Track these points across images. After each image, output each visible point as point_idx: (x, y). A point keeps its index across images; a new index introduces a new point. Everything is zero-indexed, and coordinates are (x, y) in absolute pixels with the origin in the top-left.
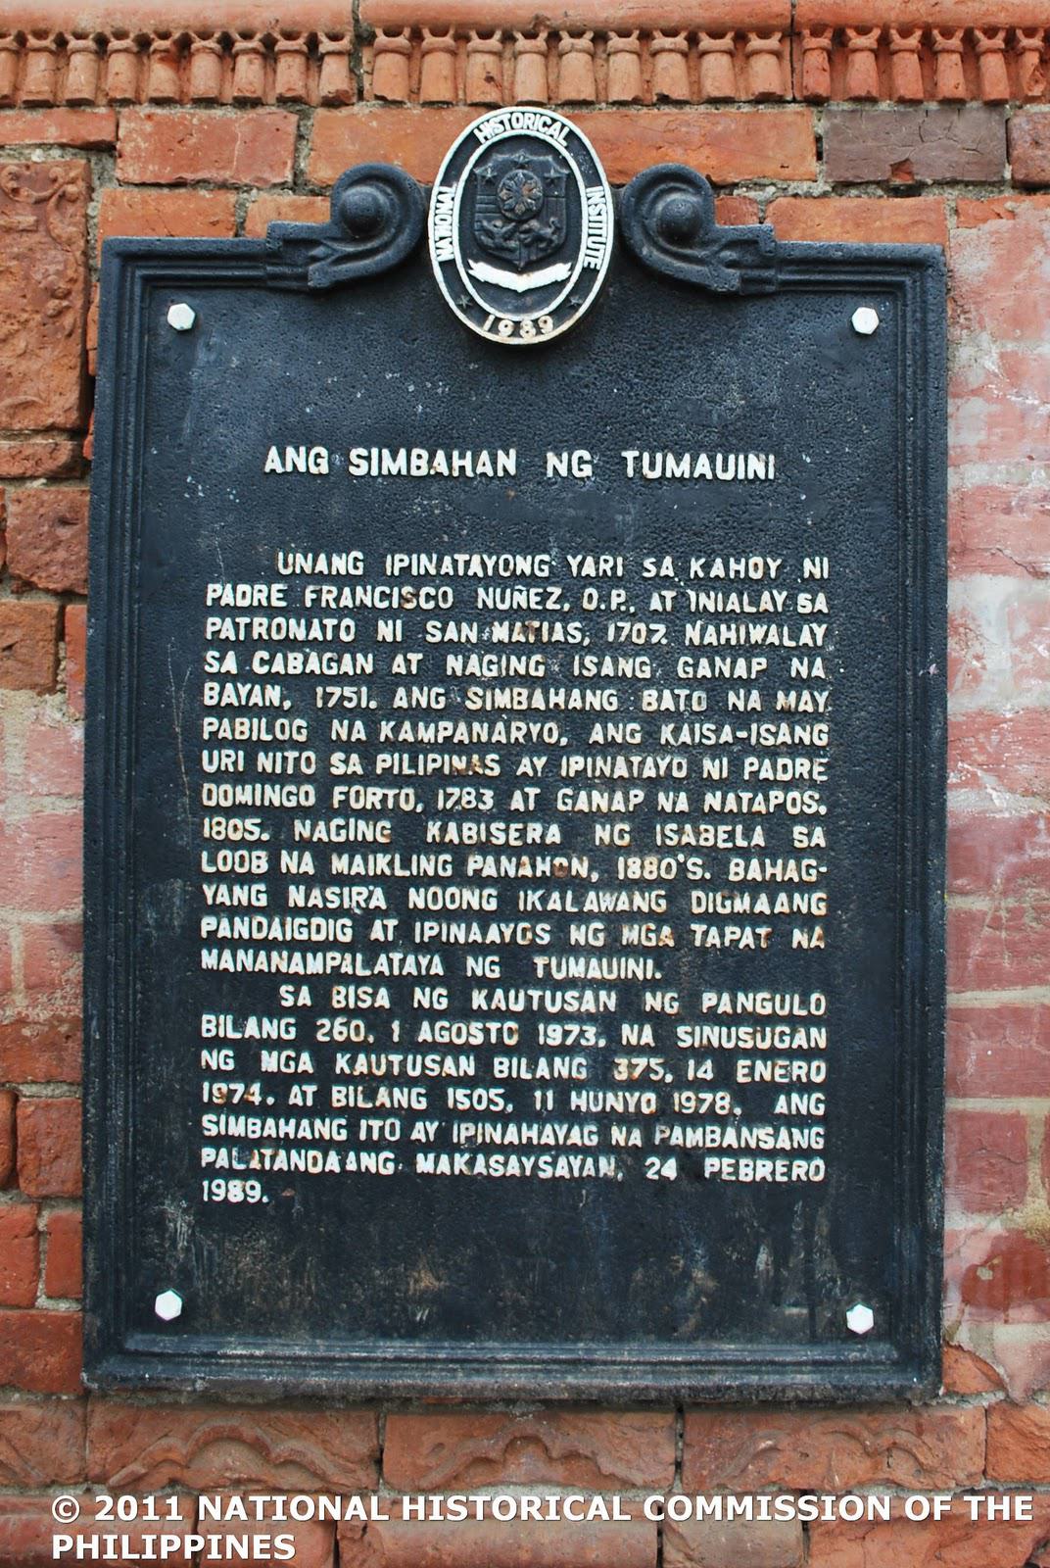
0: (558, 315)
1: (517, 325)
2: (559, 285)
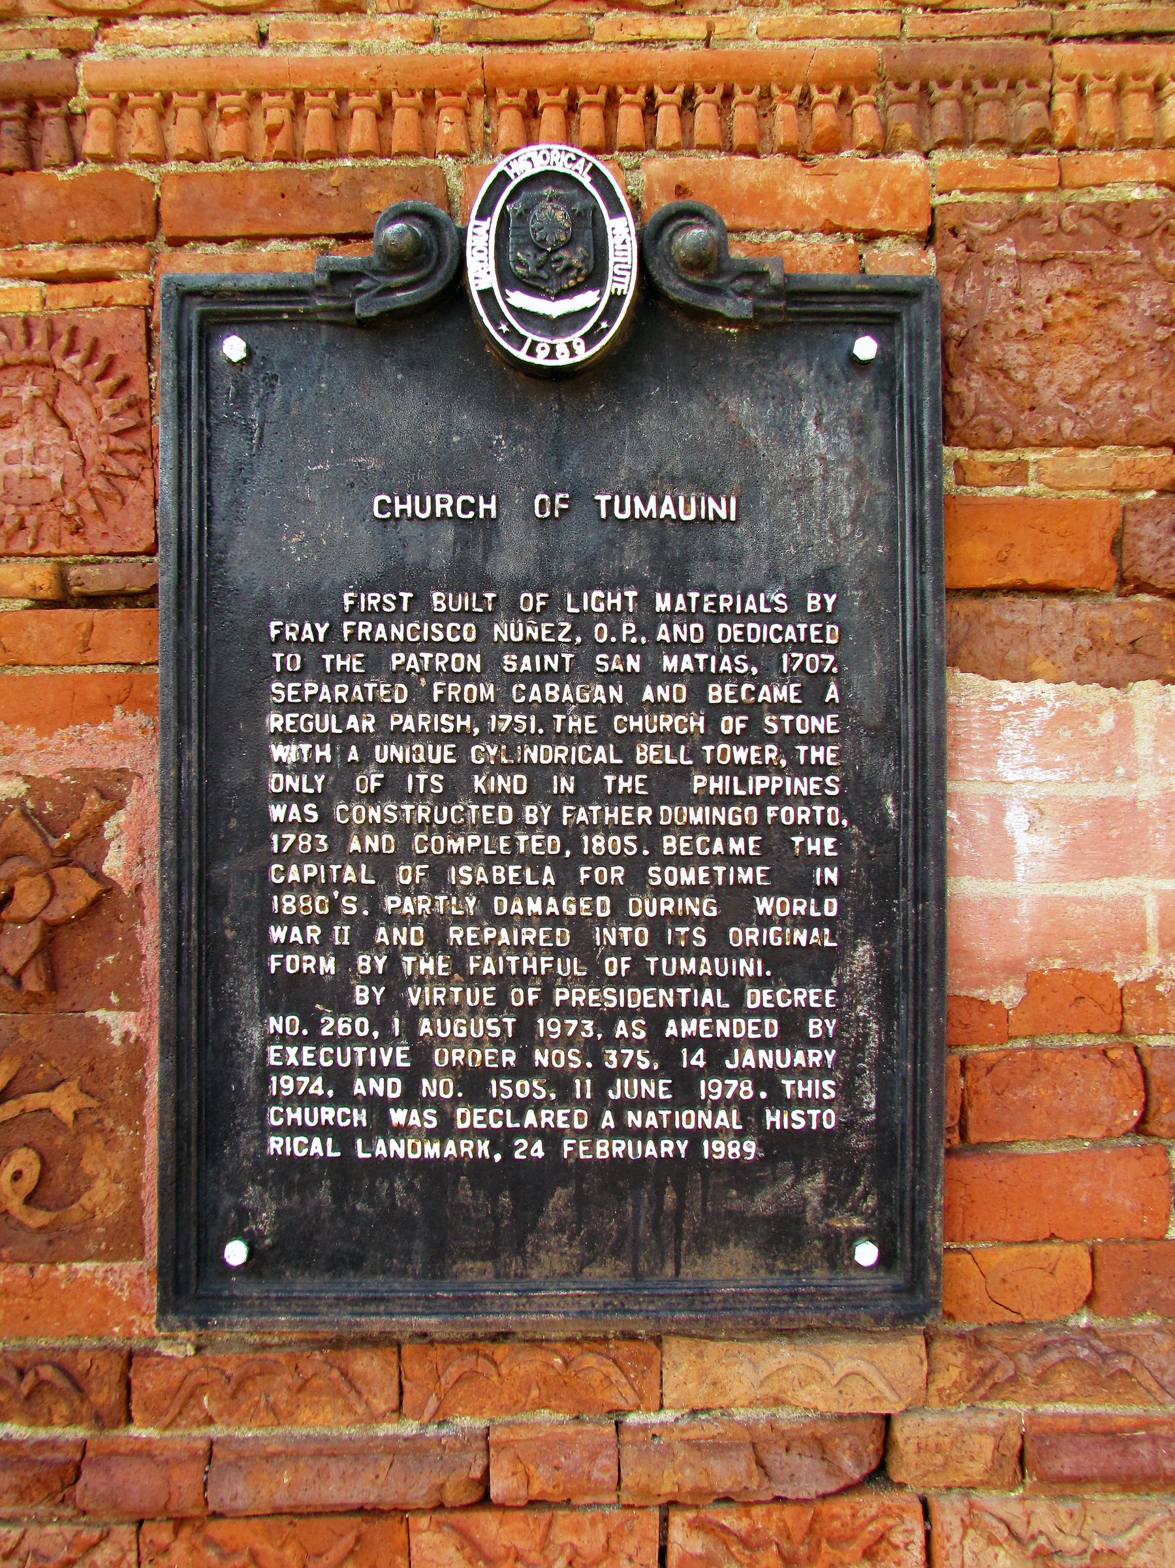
0: (590, 339)
1: (553, 347)
2: (587, 312)
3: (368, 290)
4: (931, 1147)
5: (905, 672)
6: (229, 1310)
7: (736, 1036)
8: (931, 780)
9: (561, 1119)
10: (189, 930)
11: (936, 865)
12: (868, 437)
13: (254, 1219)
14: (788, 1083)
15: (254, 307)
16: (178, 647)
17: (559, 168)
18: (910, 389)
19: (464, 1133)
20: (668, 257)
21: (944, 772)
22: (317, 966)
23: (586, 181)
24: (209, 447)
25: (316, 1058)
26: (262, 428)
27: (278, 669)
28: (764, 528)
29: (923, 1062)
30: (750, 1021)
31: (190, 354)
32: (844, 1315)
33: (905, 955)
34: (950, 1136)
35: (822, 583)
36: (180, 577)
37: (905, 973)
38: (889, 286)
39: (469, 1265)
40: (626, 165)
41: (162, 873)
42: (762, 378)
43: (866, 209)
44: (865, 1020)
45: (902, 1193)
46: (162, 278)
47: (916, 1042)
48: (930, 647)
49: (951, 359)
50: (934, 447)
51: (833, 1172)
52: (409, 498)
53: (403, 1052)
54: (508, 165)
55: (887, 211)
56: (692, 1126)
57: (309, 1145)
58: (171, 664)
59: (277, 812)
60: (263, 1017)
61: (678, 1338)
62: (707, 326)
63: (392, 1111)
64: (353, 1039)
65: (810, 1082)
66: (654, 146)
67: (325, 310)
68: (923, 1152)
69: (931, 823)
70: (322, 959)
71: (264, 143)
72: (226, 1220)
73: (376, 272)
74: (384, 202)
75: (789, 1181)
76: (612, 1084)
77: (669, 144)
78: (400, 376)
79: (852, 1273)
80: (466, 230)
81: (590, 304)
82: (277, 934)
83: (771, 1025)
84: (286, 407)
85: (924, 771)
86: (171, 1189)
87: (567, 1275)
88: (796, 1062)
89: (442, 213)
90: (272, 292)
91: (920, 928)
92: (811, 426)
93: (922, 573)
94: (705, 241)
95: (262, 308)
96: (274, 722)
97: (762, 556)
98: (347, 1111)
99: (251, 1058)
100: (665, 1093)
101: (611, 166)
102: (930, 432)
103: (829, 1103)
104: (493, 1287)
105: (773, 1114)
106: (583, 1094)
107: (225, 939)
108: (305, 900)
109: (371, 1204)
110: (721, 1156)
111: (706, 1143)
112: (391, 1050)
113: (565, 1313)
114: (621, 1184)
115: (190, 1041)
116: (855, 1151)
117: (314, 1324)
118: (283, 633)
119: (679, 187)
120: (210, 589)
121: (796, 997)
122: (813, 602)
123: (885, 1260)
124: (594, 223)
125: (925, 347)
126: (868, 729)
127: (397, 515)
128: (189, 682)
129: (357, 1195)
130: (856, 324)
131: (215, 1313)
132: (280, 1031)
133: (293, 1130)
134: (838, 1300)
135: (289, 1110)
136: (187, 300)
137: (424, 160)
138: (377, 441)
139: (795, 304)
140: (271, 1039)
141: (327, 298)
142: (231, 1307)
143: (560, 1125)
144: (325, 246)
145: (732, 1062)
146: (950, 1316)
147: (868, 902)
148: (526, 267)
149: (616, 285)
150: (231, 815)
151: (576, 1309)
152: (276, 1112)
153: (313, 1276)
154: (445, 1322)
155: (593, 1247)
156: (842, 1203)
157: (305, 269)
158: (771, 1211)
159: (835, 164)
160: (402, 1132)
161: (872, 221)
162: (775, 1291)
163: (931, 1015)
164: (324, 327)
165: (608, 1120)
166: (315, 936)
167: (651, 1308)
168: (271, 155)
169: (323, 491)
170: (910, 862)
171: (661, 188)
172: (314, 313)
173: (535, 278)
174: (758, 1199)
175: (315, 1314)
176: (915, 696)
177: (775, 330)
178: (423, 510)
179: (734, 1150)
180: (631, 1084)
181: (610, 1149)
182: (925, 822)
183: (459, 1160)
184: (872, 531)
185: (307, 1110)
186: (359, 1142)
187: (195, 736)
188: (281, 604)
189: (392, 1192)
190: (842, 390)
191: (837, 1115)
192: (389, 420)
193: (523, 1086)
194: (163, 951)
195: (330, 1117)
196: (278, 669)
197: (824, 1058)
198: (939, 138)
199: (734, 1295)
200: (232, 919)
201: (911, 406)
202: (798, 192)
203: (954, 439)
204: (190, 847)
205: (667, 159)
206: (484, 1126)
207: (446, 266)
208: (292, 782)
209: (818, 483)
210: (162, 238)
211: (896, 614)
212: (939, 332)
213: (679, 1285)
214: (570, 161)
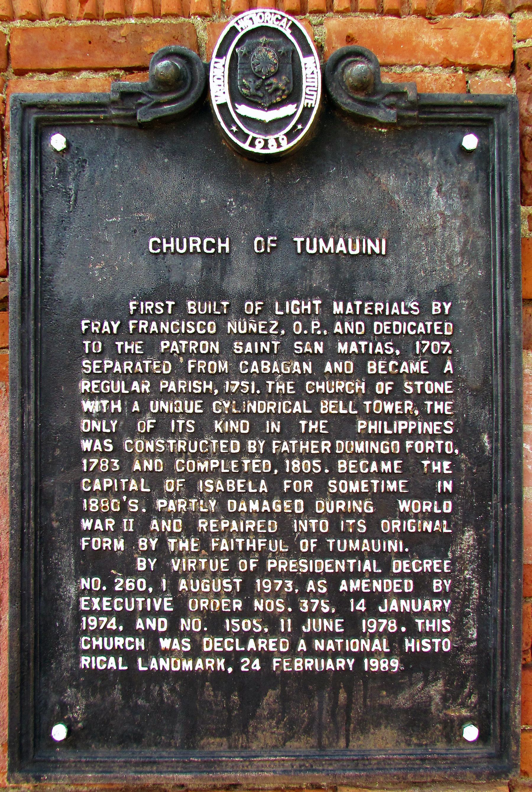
0: (290, 136)
1: (266, 141)
2: (288, 118)
3: (146, 104)
4: (513, 663)
5: (496, 353)
6: (54, 769)
7: (386, 590)
8: (513, 424)
9: (271, 645)
10: (29, 522)
11: (516, 479)
12: (471, 200)
13: (71, 710)
14: (419, 622)
15: (71, 115)
16: (22, 337)
17: (270, 25)
18: (499, 169)
19: (209, 654)
20: (341, 83)
21: (521, 418)
22: (112, 545)
23: (288, 32)
24: (42, 206)
25: (112, 605)
26: (76, 194)
27: (87, 351)
28: (404, 259)
29: (507, 608)
30: (395, 581)
31: (29, 146)
32: (456, 773)
33: (496, 538)
34: (525, 656)
35: (442, 296)
36: (23, 291)
37: (496, 550)
38: (486, 101)
39: (212, 740)
40: (314, 22)
41: (11, 484)
42: (403, 161)
43: (471, 51)
44: (470, 580)
45: (494, 693)
46: (11, 96)
47: (503, 594)
48: (512, 337)
49: (526, 149)
50: (515, 207)
51: (449, 680)
52: (172, 239)
53: (168, 601)
54: (237, 23)
55: (484, 52)
56: (357, 650)
57: (107, 662)
58: (17, 348)
59: (86, 445)
60: (77, 579)
61: (348, 788)
62: (367, 127)
63: (161, 639)
64: (136, 593)
65: (434, 621)
66: (332, 10)
67: (117, 117)
68: (508, 666)
69: (513, 452)
70: (115, 541)
71: (77, 8)
72: (53, 711)
73: (151, 92)
74: (156, 47)
75: (420, 685)
76: (305, 622)
77: (342, 9)
78: (166, 160)
79: (461, 745)
80: (209, 65)
81: (290, 114)
82: (86, 524)
83: (409, 584)
84: (92, 180)
85: (508, 417)
86: (17, 690)
87: (275, 747)
88: (425, 608)
89: (194, 54)
90: (83, 105)
91: (506, 520)
92: (434, 193)
93: (507, 289)
94: (366, 72)
95: (76, 115)
96: (84, 386)
97: (402, 277)
98: (132, 640)
99: (69, 605)
100: (339, 628)
101: (304, 23)
102: (513, 197)
103: (446, 635)
104: (228, 754)
105: (410, 642)
106: (286, 628)
107: (52, 527)
108: (105, 502)
109: (148, 700)
110: (376, 669)
111: (366, 661)
112: (160, 600)
113: (274, 772)
114: (310, 687)
115: (29, 594)
116: (463, 666)
117: (111, 778)
118: (90, 328)
119: (348, 37)
120: (42, 299)
121: (425, 565)
122: (436, 308)
123: (483, 737)
124: (293, 60)
125: (509, 141)
126: (472, 390)
127: (165, 251)
128: (29, 360)
129: (138, 694)
130: (464, 126)
131: (45, 772)
132: (88, 588)
133: (96, 652)
134: (452, 763)
135: (94, 639)
136: (27, 110)
137: (182, 19)
138: (151, 202)
139: (424, 113)
140: (82, 592)
141: (119, 109)
142: (56, 767)
143: (271, 649)
144: (117, 76)
145: (383, 608)
146: (525, 773)
147: (472, 503)
148: (249, 89)
149: (307, 101)
150: (56, 446)
151: (281, 768)
152: (86, 640)
153: (109, 748)
154: (196, 777)
155: (293, 729)
156: (455, 699)
157: (104, 91)
158: (408, 705)
159: (450, 22)
160: (168, 653)
161: (474, 59)
162: (411, 757)
163: (513, 577)
164: (117, 128)
165: (302, 645)
166: (111, 526)
167: (330, 768)
168: (82, 16)
169: (116, 235)
170: (499, 477)
171: (337, 37)
172: (110, 119)
173: (254, 96)
174: (400, 697)
175: (111, 772)
176: (503, 369)
177: (411, 130)
178: (181, 247)
179: (384, 665)
180: (317, 622)
181: (303, 665)
182: (509, 451)
183: (205, 672)
184: (474, 262)
185: (106, 639)
186: (140, 660)
187: (32, 395)
188: (89, 309)
189: (161, 690)
190: (455, 170)
191: (452, 642)
192: (160, 189)
193: (246, 623)
194: (11, 536)
195: (121, 644)
196: (87, 351)
197: (443, 605)
198: (518, 5)
199: (384, 760)
200: (57, 514)
201: (500, 180)
202: (426, 40)
203: (528, 201)
204: (29, 467)
205: (341, 19)
206: (221, 649)
207: (196, 88)
208: (96, 425)
209: (439, 230)
210: (11, 70)
211: (490, 315)
212: (518, 131)
213: (349, 753)
214: (277, 20)
